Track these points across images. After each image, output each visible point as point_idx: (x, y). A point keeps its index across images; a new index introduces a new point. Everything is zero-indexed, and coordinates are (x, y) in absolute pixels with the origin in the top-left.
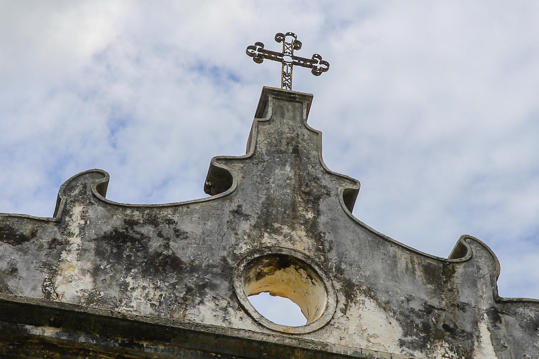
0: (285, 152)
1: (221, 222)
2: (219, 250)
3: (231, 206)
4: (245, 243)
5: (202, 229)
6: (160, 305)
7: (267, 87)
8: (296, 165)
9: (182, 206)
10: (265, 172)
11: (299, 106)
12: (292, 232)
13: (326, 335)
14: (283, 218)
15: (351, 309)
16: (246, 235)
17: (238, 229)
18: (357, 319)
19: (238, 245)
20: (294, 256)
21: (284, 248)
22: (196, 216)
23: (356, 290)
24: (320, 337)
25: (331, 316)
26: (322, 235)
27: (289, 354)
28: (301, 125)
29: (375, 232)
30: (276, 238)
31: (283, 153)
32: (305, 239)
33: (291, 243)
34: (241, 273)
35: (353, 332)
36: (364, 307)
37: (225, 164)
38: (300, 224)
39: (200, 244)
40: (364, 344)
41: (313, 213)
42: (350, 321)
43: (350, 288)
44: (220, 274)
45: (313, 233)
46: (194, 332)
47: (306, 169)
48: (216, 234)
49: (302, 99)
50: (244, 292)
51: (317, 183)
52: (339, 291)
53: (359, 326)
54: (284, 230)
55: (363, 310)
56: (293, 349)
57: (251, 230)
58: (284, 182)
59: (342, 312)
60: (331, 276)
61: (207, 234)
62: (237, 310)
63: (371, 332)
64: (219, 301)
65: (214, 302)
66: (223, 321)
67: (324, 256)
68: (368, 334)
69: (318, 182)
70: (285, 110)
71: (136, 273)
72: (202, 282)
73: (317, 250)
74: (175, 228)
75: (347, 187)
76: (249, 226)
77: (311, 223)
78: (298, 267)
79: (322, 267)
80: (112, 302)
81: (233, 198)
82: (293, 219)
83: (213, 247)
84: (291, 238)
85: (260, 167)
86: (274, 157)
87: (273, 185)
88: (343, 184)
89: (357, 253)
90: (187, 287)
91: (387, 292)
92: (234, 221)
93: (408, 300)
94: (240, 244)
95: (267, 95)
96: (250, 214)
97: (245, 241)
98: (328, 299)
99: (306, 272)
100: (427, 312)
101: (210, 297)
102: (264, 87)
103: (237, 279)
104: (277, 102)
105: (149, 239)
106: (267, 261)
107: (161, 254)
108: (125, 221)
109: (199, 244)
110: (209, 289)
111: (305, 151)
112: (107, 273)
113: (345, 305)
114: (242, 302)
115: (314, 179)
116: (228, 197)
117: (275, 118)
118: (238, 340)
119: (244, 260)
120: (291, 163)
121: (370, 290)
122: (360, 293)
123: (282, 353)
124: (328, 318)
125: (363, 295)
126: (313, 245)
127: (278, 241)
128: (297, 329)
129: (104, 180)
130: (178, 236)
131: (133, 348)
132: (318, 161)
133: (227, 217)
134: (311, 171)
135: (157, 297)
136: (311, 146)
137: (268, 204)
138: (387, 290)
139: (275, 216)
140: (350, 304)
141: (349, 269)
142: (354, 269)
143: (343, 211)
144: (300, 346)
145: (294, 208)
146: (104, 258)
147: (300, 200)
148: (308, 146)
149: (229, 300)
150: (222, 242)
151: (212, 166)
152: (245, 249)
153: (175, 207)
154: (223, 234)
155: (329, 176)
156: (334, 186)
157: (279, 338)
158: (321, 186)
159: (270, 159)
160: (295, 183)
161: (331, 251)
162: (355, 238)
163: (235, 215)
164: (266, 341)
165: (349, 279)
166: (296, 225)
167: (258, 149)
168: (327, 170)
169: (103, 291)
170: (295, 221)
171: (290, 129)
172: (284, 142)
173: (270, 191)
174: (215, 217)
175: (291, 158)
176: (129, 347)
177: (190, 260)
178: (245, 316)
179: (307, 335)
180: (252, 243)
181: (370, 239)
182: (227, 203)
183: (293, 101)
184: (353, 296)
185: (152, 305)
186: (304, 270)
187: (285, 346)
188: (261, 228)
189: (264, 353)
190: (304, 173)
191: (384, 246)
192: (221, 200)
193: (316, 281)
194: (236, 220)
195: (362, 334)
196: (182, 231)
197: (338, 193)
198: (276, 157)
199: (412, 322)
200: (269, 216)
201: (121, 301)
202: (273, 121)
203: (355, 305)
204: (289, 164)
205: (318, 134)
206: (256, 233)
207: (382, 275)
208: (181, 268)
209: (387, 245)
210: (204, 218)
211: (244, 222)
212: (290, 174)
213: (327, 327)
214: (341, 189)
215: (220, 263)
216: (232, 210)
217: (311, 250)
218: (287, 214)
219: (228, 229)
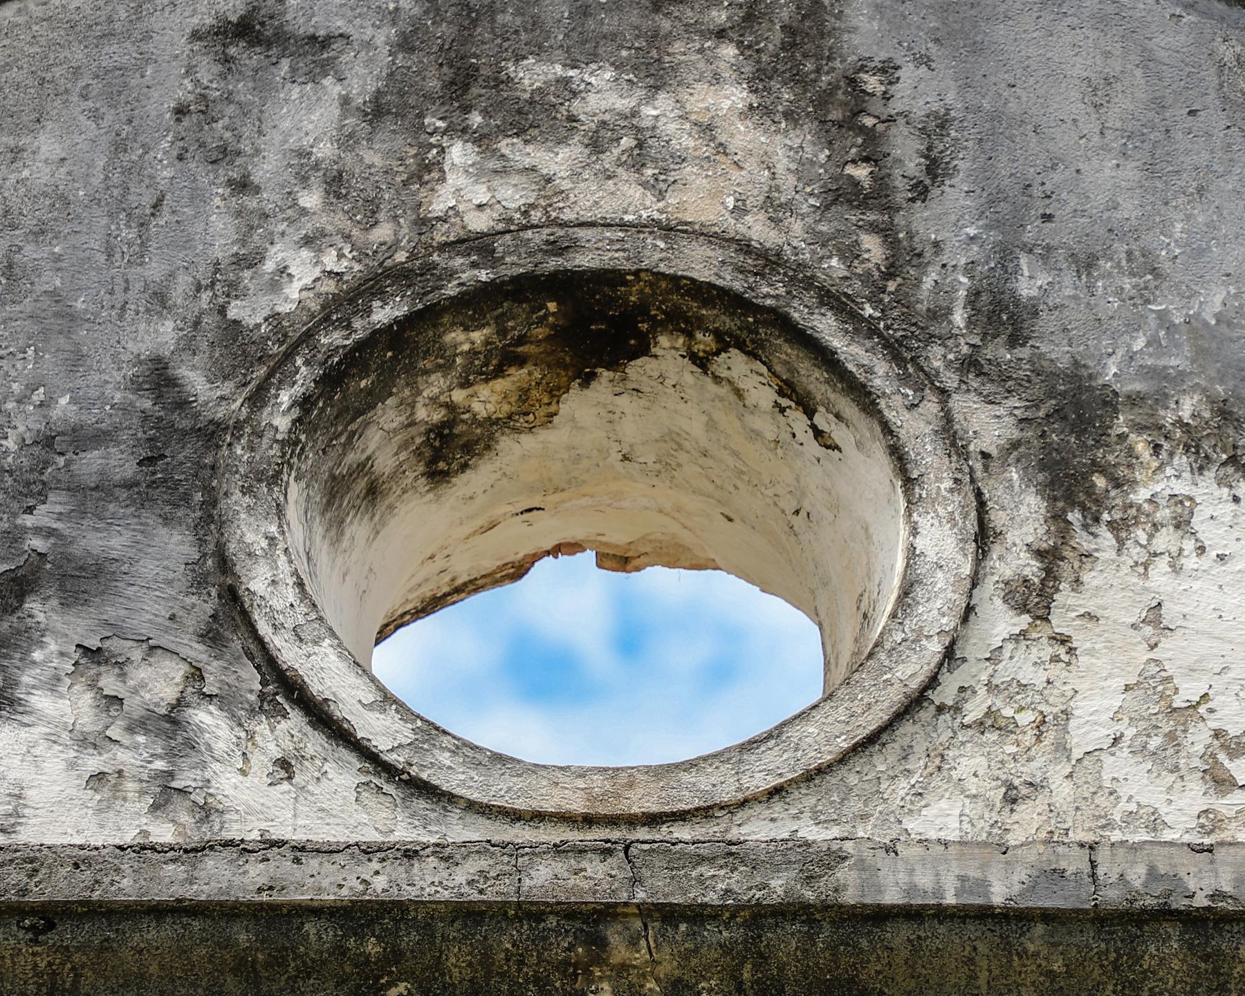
1: (130, 121)
2: (121, 317)
4: (308, 241)
12: (650, 99)
13: (903, 785)
15: (1086, 577)
16: (316, 179)
17: (257, 151)
18: (1136, 636)
19: (251, 261)
20: (663, 268)
21: (592, 224)
23: (1122, 437)
24: (855, 805)
25: (935, 648)
26: (872, 83)
30: (527, 162)
33: (645, 185)
34: (275, 450)
36: (1189, 545)
38: (706, 34)
42: (1084, 660)
43: (1081, 426)
44: (128, 485)
45: (797, 79)
48: (97, 211)
50: (300, 584)
52: (995, 466)
54: (592, 99)
55: (1176, 569)
57: (347, 141)
59: (1023, 608)
60: (936, 364)
61: (29, 222)
62: (252, 712)
64: (123, 676)
65: (93, 685)
66: (155, 807)
67: (886, 232)
68: (1217, 734)
76: (337, 112)
77: (785, 14)
78: (705, 341)
79: (868, 311)
83: (79, 305)
84: (640, 145)
89: (1131, 172)
92: (229, 98)
96: (340, 25)
97: (307, 227)
98: (914, 532)
99: (764, 370)
101: (62, 654)
103: (247, 499)
106: (478, 336)
110: (54, 602)
113: (1040, 554)
114: (289, 654)
119: (299, 361)
122: (1157, 448)
125: (1181, 460)
126: (802, 169)
127: (549, 181)
128: (686, 777)
140: (1082, 540)
141: (1069, 292)
149: (198, 652)
150: (139, 259)
152: (308, 280)
154: (148, 199)
161: (935, 192)
162: (1116, 66)
163: (232, 51)
165: (1076, 363)
166: (678, 47)
170: (666, 25)
174: (85, 97)
178: (315, 742)
179: (758, 808)
180: (355, 232)
184: (1100, 482)
186: (753, 355)
188: (421, 116)
193: (838, 416)
194: (242, 90)
195: (1171, 736)
200: (475, 22)
203: (1121, 542)
206: (387, 154)
211: (295, 95)
213: (907, 728)
215: (125, 409)
216: (209, 21)
217: (789, 207)
219: (180, 158)
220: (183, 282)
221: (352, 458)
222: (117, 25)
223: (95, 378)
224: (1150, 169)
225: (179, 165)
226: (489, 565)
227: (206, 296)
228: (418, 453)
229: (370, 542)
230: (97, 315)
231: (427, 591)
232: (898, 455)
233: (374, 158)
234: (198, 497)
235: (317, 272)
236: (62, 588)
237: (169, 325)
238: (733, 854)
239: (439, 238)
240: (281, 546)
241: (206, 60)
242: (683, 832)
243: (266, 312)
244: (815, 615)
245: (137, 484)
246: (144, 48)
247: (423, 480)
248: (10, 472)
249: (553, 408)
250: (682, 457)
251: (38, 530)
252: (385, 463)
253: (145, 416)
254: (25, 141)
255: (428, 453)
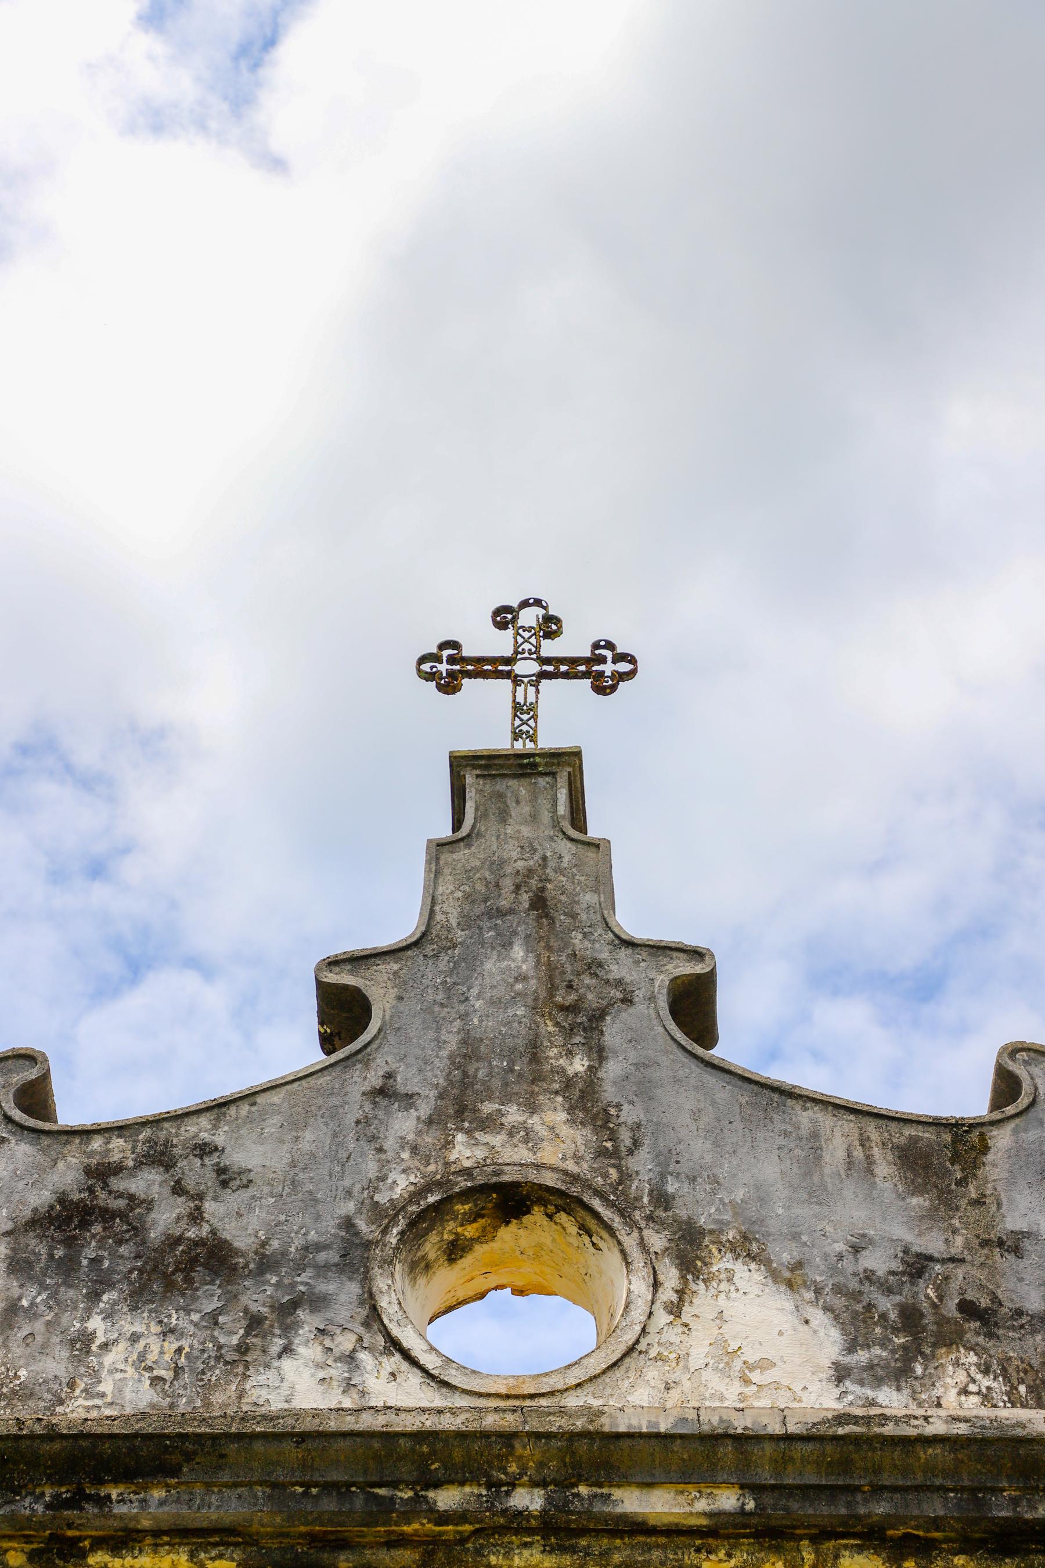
0: (511, 911)
2: (334, 1200)
3: (366, 1077)
4: (404, 1171)
5: (290, 1152)
6: (176, 1376)
7: (458, 751)
8: (540, 939)
9: (238, 1104)
10: (455, 972)
11: (548, 783)
12: (531, 1117)
13: (626, 1382)
14: (506, 1084)
15: (694, 1301)
17: (386, 1137)
19: (382, 1179)
20: (535, 1181)
21: (509, 1164)
22: (275, 1121)
23: (707, 1246)
24: (608, 1391)
25: (638, 1328)
26: (612, 1111)
27: (499, 1455)
28: (552, 833)
29: (757, 1078)
30: (485, 1141)
31: (505, 915)
32: (565, 1131)
33: (529, 1149)
34: (391, 1252)
35: (701, 1363)
36: (733, 1288)
37: (352, 972)
39: (284, 1194)
40: (731, 1393)
41: (586, 1058)
43: (691, 1242)
44: (336, 1265)
45: (585, 1110)
46: (239, 1437)
47: (567, 944)
49: (553, 764)
50: (400, 1304)
51: (597, 975)
52: (659, 1257)
53: (719, 1343)
54: (509, 1117)
55: (728, 1298)
56: (508, 1438)
57: (419, 1133)
58: (509, 989)
59: (671, 1313)
60: (637, 1218)
61: (301, 1165)
62: (381, 1354)
63: (751, 1355)
64: (333, 1340)
65: (321, 1343)
66: (344, 1392)
67: (618, 1168)
68: (745, 1362)
69: (600, 974)
70: (509, 802)
71: (115, 1303)
72: (289, 1294)
73: (599, 1156)
74: (218, 1163)
75: (677, 972)
77: (580, 1085)
78: (551, 1209)
79: (612, 1197)
80: (48, 1391)
81: (371, 1057)
82: (533, 1082)
83: (319, 1196)
84: (527, 1134)
85: (445, 962)
86: (480, 928)
87: (477, 1005)
88: (667, 967)
89: (708, 1145)
90: (249, 1315)
91: (796, 1236)
92: (375, 1117)
93: (856, 1250)
94: (391, 1174)
95: (462, 773)
96: (417, 1089)
97: (404, 1166)
98: (630, 1283)
99: (573, 1220)
100: (911, 1275)
101: (310, 1331)
102: (450, 752)
104: (488, 786)
105: (149, 1204)
106: (467, 1207)
107: (179, 1240)
108: (88, 1171)
109: (281, 1196)
110: (308, 1311)
111: (563, 898)
112: (36, 1316)
113: (677, 1292)
114: (395, 1331)
115: (590, 968)
116: (360, 1056)
117: (483, 829)
118: (358, 1440)
119: (400, 1217)
120: (528, 936)
121: (745, 1237)
122: (720, 1250)
123: (482, 1455)
124: (629, 1337)
125: (729, 1255)
128: (545, 1379)
129: (33, 1074)
130: (224, 1184)
131: (82, 1509)
132: (599, 917)
133: (355, 1108)
134: (581, 946)
135: (167, 1358)
136: (579, 883)
137: (465, 1056)
138: (794, 1229)
139: (483, 1083)
140: (692, 1286)
142: (703, 1188)
143: (668, 1038)
144: (527, 1428)
145: (535, 1054)
146: (30, 1278)
147: (551, 1029)
148: (573, 883)
149: (361, 1330)
151: (320, 985)
152: (404, 1186)
153: (220, 1107)
154: (345, 1155)
155: (630, 951)
156: (644, 975)
157: (467, 1415)
158: (608, 982)
159: (471, 938)
160: (537, 989)
161: (636, 1152)
163: (377, 1099)
164: (434, 1428)
166: (541, 1097)
167: (439, 917)
168: (624, 937)
169: (26, 1365)
170: (537, 1089)
171: (522, 847)
172: (508, 884)
173: (472, 1020)
174: (322, 1117)
175: (527, 924)
176: (72, 1508)
177: (257, 1241)
178: (405, 1366)
179: (572, 1392)
180: (422, 1168)
181: (743, 1100)
182: (356, 1073)
183: (530, 775)
184: (699, 1263)
185: (156, 1380)
186: (569, 1214)
187: (485, 1435)
188: (446, 1124)
189: (432, 1463)
190: (560, 956)
191: (784, 1112)
192: (338, 1069)
193: (601, 1238)
194: (381, 1114)
195: (727, 1363)
196: (236, 1168)
197: (653, 992)
198: (485, 929)
199: (870, 1307)
200: (466, 1088)
201: (72, 1385)
202: (479, 835)
203: (707, 1287)
204: (520, 942)
205: (598, 846)
206: (434, 1138)
207: (780, 1193)
208: (234, 1268)
209: (792, 1108)
210: (295, 1125)
211: (400, 1116)
212: (524, 967)
213: (628, 1360)
214: (662, 981)
215: (335, 1236)
216: (369, 1088)
217: (582, 1158)
218: (516, 1074)
219: (357, 1140)
220: (358, 1187)
221: (420, 1254)
222: (335, 1090)
223: (324, 1224)
224: (715, 1144)
225: (357, 1142)
226: (471, 1294)
227: (366, 1192)
228: (444, 1252)
229: (426, 1286)
230: (325, 1200)
231: (447, 1304)
232: (623, 1253)
233: (429, 1139)
234: (362, 1269)
235: (407, 1183)
236: (311, 1306)
237: (352, 1203)
238: (562, 1411)
239: (453, 1170)
240: (393, 1289)
241: (367, 1103)
242: (544, 1402)
243: (388, 1198)
244: (593, 1314)
245: (339, 1265)
246: (345, 1098)
247: (446, 1262)
248: (292, 1261)
249: (495, 1234)
250: (543, 1253)
251: (302, 1283)
252: (432, 1256)
253: (343, 1238)
254: (300, 1134)
255: (448, 1252)
